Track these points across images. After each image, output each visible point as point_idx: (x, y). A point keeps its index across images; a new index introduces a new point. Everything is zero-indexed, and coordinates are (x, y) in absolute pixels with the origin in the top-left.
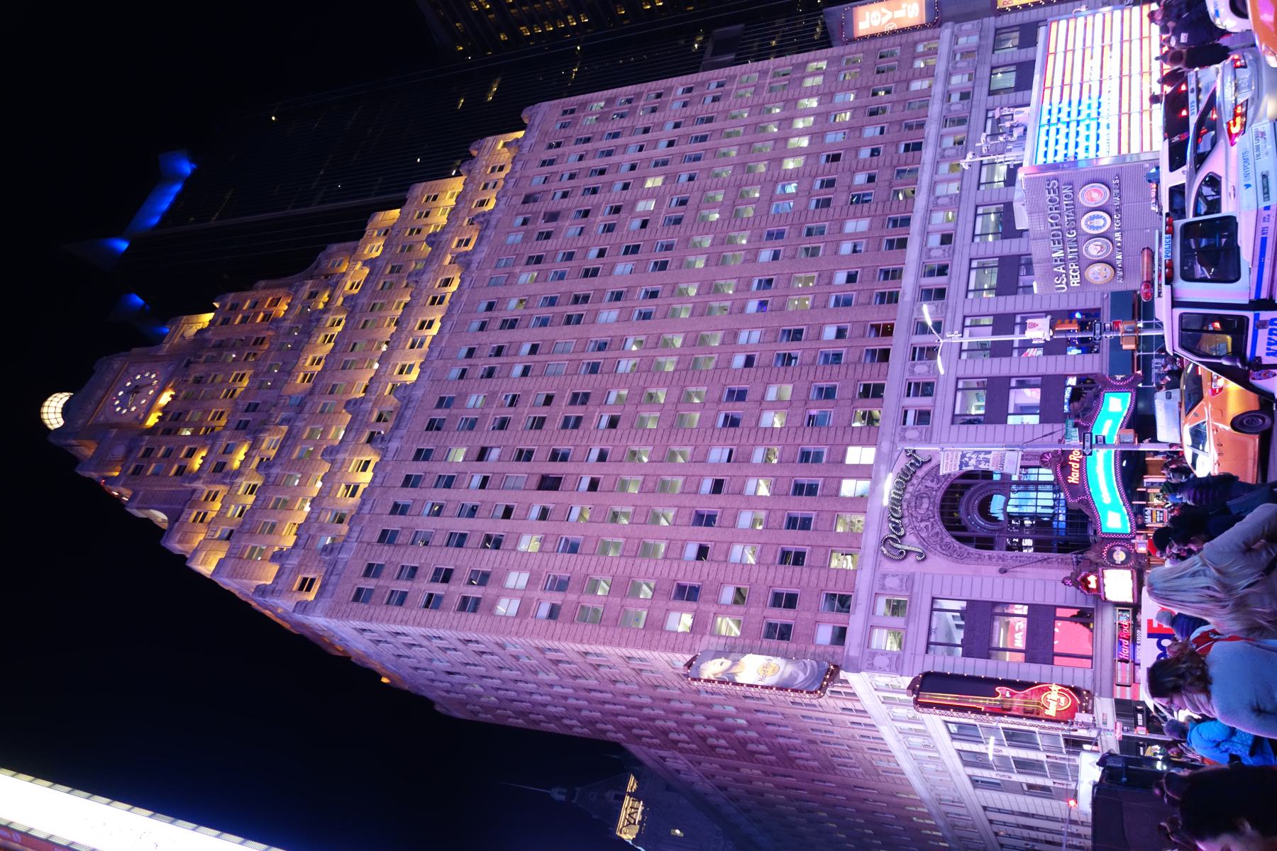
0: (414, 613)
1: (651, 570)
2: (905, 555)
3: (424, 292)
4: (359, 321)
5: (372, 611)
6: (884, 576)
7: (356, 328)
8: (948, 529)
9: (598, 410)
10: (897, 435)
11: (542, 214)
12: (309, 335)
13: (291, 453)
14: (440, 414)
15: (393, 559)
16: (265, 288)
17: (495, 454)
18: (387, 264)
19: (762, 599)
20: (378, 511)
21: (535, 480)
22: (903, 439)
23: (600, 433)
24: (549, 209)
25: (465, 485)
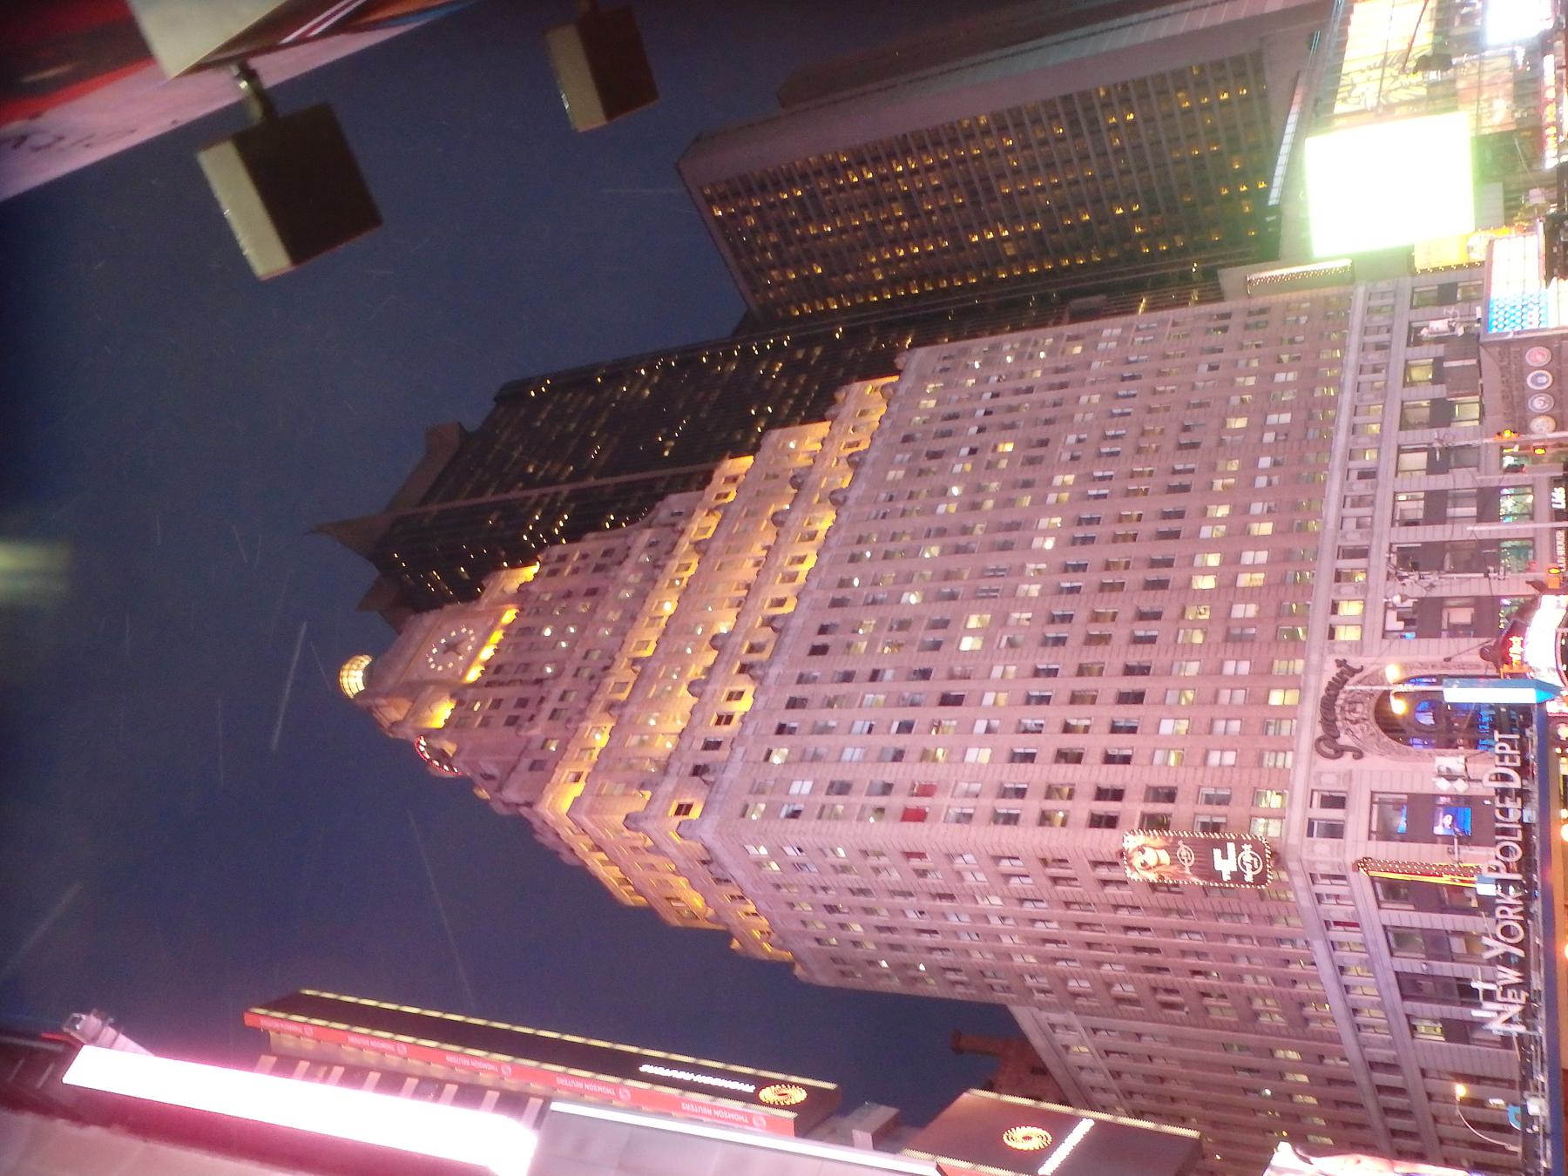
0: (813, 823)
1: (1069, 775)
2: (1339, 752)
3: (792, 532)
4: (715, 564)
5: (765, 824)
6: (1320, 774)
7: (712, 570)
8: (1385, 731)
9: (1000, 631)
10: (1326, 649)
11: (924, 453)
12: (655, 581)
13: (648, 693)
14: (822, 640)
15: (784, 776)
16: (596, 539)
17: (889, 675)
18: (743, 508)
19: (1191, 797)
20: (763, 732)
21: (936, 698)
22: (1332, 651)
23: (1004, 652)
24: (933, 449)
25: (858, 704)
